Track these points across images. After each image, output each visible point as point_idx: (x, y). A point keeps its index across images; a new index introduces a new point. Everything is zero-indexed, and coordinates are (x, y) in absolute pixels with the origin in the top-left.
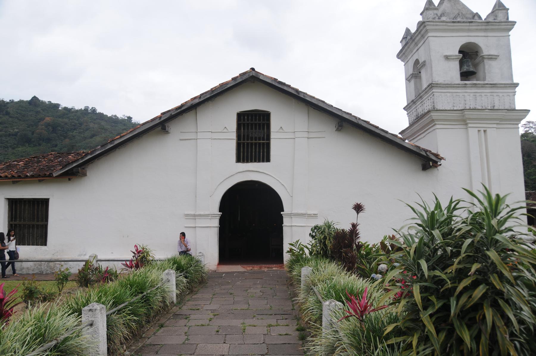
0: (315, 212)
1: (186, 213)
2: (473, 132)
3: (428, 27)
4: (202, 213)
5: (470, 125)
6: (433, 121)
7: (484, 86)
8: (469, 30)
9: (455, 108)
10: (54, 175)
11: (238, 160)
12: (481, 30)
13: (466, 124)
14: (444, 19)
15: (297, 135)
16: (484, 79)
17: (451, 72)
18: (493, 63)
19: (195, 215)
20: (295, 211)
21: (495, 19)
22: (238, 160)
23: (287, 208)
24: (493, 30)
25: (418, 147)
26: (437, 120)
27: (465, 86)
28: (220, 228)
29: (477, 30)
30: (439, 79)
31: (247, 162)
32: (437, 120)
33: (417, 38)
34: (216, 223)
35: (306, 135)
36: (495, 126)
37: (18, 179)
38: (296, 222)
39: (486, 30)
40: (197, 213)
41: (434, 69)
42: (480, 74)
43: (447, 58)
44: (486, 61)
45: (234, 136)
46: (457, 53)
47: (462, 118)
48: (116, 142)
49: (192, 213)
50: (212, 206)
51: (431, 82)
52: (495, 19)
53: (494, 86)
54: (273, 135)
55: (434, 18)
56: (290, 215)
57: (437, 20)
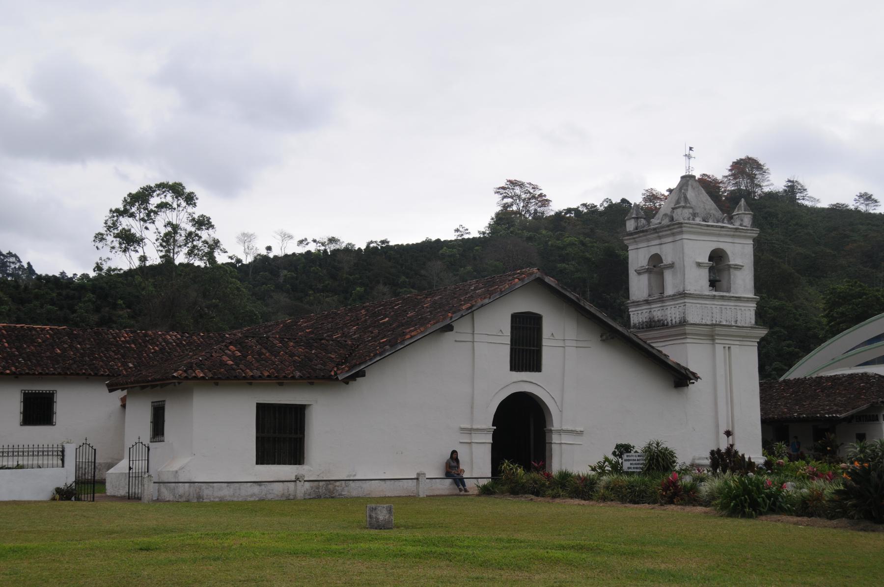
0: (582, 429)
1: (463, 426)
2: (719, 349)
3: (684, 229)
4: (479, 427)
5: (717, 341)
6: (685, 334)
7: (730, 299)
8: (720, 235)
9: (704, 322)
10: (340, 378)
11: (511, 370)
12: (729, 235)
13: (713, 340)
14: (698, 220)
15: (568, 343)
16: (728, 291)
17: (697, 280)
18: (738, 273)
19: (471, 430)
20: (564, 428)
21: (741, 225)
22: (511, 370)
23: (556, 425)
24: (739, 237)
25: (679, 364)
26: (689, 334)
27: (714, 297)
28: (492, 444)
29: (726, 235)
30: (691, 289)
31: (522, 371)
32: (689, 334)
33: (664, 233)
34: (489, 439)
35: (574, 344)
36: (738, 343)
37: (281, 381)
38: (565, 439)
39: (733, 236)
40: (475, 427)
41: (686, 276)
42: (724, 283)
43: (699, 265)
44: (732, 270)
45: (508, 340)
46: (707, 261)
47: (712, 332)
48: (407, 343)
49: (469, 426)
50: (486, 420)
51: (681, 290)
52: (741, 225)
53: (739, 299)
54: (545, 342)
55: (689, 219)
56: (560, 432)
57: (691, 222)
